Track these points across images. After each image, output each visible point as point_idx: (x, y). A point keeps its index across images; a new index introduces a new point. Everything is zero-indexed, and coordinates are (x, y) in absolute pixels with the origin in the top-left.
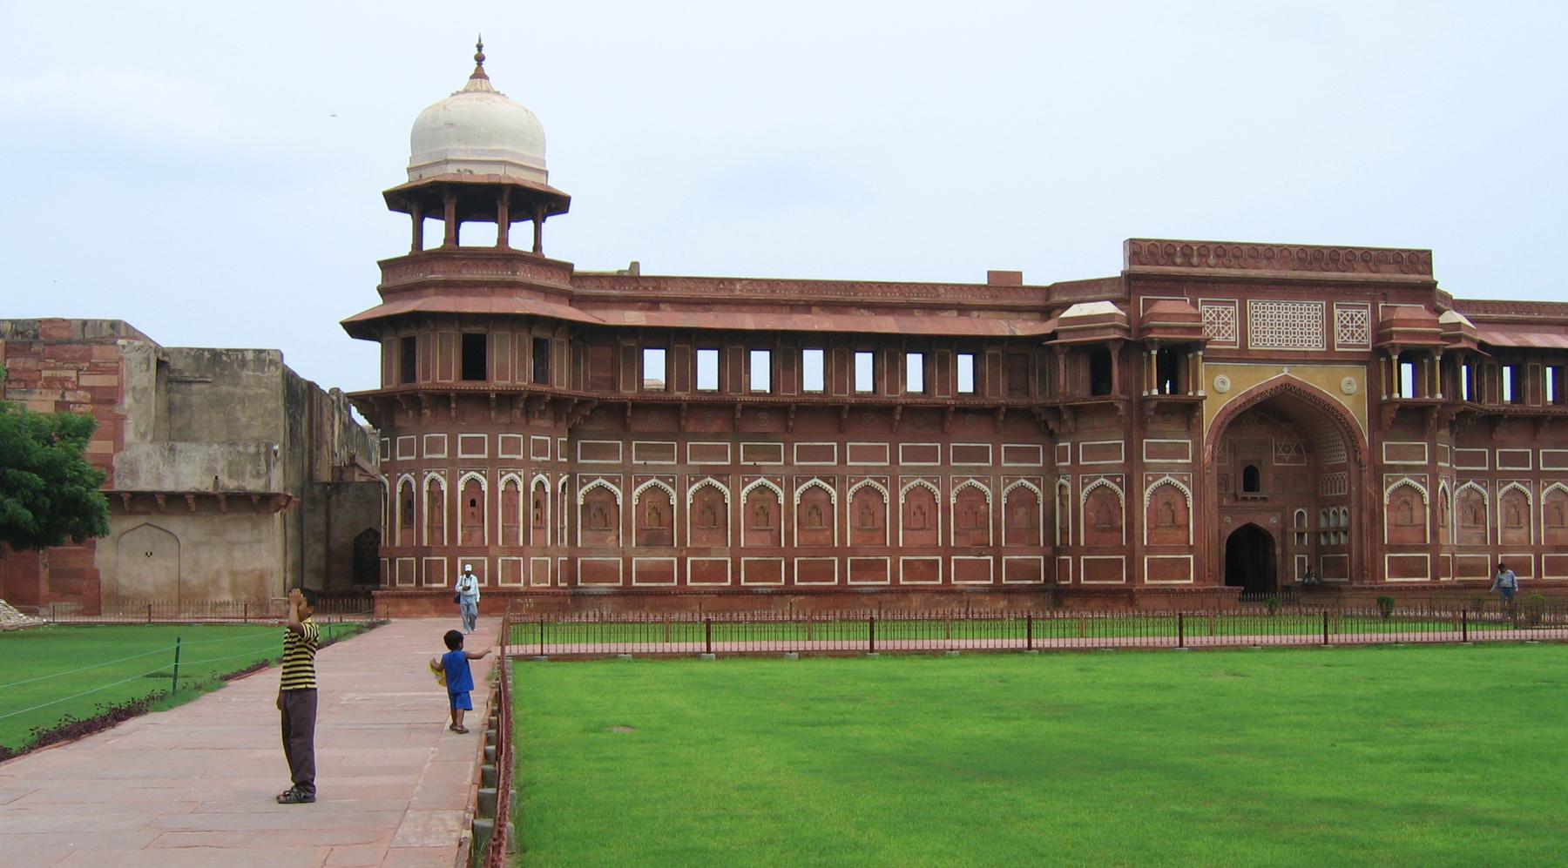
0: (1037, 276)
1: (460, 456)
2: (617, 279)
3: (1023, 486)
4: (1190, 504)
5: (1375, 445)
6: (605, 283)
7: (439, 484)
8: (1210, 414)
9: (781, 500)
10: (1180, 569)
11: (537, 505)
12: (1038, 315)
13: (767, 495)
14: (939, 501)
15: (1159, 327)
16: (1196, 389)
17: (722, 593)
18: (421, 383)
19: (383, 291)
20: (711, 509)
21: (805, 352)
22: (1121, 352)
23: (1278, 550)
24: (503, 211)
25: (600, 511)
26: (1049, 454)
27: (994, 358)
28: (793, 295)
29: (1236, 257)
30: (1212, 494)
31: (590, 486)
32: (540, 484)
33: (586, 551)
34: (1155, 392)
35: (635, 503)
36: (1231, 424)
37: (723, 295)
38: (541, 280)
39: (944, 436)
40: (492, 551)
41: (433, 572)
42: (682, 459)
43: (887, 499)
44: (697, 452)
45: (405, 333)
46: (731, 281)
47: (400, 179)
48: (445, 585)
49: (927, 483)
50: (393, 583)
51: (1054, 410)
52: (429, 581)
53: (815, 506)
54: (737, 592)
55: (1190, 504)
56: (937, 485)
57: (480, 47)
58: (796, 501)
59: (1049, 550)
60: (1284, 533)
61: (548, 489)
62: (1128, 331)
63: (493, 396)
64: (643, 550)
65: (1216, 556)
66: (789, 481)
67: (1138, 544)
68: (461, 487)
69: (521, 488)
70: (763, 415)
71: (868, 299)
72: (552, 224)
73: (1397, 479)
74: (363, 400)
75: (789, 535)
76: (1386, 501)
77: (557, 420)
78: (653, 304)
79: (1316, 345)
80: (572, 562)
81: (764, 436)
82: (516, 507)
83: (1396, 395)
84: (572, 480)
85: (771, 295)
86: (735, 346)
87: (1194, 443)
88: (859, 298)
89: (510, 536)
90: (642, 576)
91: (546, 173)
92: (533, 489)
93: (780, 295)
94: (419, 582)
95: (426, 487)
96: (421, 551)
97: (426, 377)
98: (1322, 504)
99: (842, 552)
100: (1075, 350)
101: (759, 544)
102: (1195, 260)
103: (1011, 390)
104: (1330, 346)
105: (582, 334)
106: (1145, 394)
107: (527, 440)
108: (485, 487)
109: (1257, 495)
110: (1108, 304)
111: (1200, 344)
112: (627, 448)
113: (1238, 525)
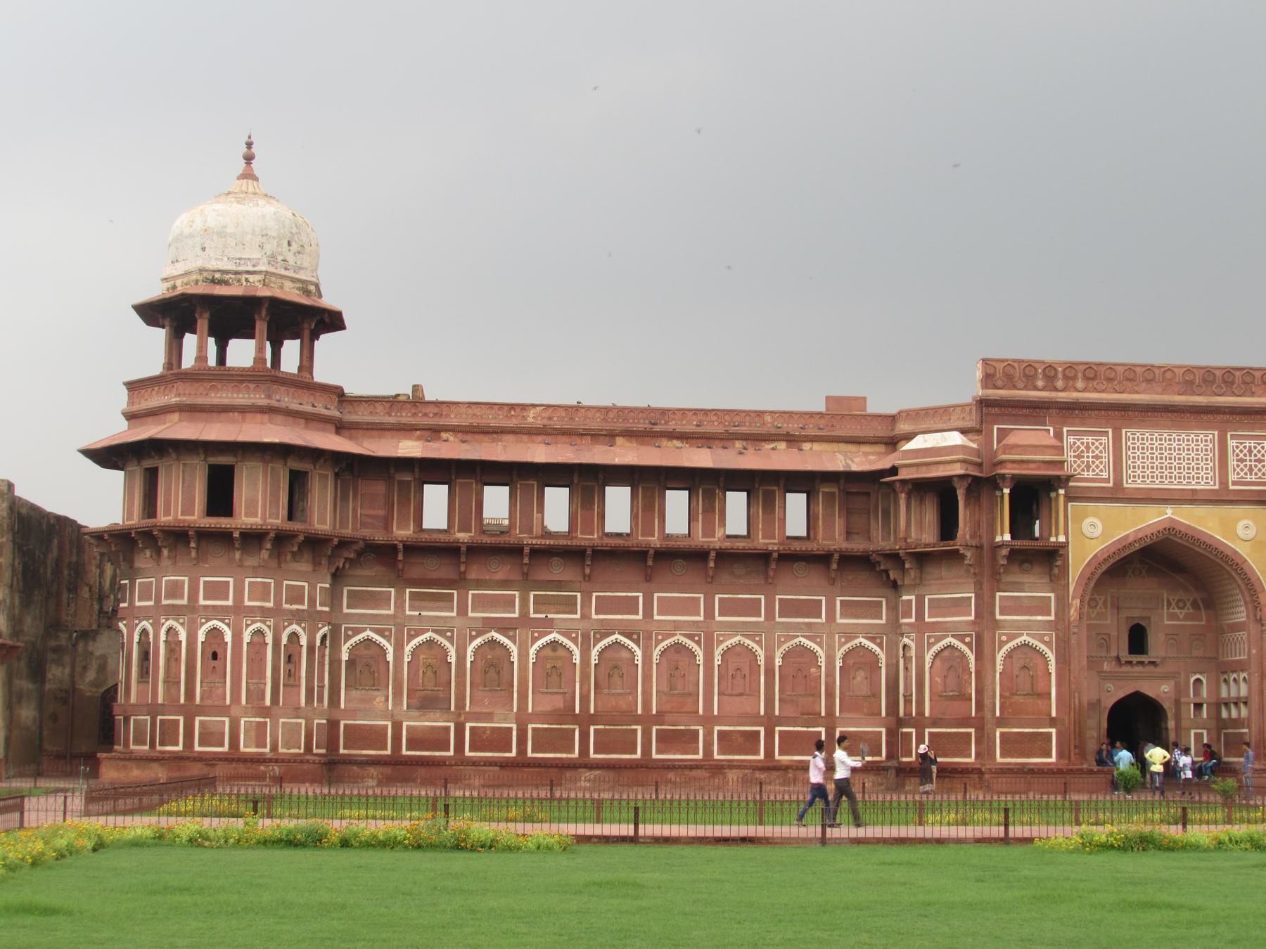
0: (883, 401)
1: (202, 602)
2: (393, 402)
3: (861, 646)
4: (1052, 668)
6: (379, 408)
7: (177, 633)
8: (1079, 562)
9: (577, 658)
10: (1039, 744)
11: (289, 659)
12: (881, 448)
13: (561, 652)
14: (762, 663)
15: (1013, 462)
16: (1057, 536)
17: (505, 764)
18: (163, 518)
19: (131, 416)
20: (493, 667)
21: (610, 491)
22: (969, 491)
23: (1171, 724)
24: (261, 327)
25: (367, 667)
26: (893, 608)
27: (829, 497)
28: (595, 424)
29: (1110, 380)
30: (1079, 660)
31: (356, 639)
32: (294, 637)
33: (351, 713)
34: (1007, 537)
35: (407, 659)
36: (1104, 573)
37: (511, 423)
38: (305, 405)
39: (769, 586)
40: (235, 711)
41: (169, 733)
42: (462, 611)
43: (700, 659)
44: (480, 603)
45: (148, 463)
46: (524, 407)
47: (155, 291)
48: (180, 748)
49: (747, 642)
50: (127, 744)
51: (894, 557)
52: (162, 744)
53: (614, 667)
54: (521, 763)
55: (1052, 668)
56: (759, 643)
57: (249, 145)
58: (594, 659)
59: (892, 719)
60: (1177, 703)
61: (304, 641)
62: (979, 465)
63: (236, 535)
64: (416, 713)
65: (1096, 727)
66: (586, 637)
67: (988, 715)
68: (201, 637)
69: (269, 639)
70: (555, 560)
71: (679, 429)
72: (326, 343)
74: (99, 536)
75: (585, 699)
77: (316, 564)
78: (435, 432)
79: (1206, 482)
80: (333, 725)
81: (559, 585)
82: (263, 660)
84: (335, 631)
85: (649, 424)
86: (527, 478)
87: (1057, 598)
88: (671, 426)
89: (256, 695)
90: (412, 744)
91: (317, 286)
92: (284, 640)
93: (578, 423)
94: (153, 745)
95: (163, 637)
96: (154, 710)
97: (167, 513)
98: (1223, 669)
99: (647, 720)
100: (920, 488)
101: (549, 708)
102: (1060, 384)
103: (849, 534)
105: (352, 468)
106: (998, 539)
107: (278, 586)
108: (228, 638)
110: (956, 434)
111: (1062, 481)
112: (400, 597)
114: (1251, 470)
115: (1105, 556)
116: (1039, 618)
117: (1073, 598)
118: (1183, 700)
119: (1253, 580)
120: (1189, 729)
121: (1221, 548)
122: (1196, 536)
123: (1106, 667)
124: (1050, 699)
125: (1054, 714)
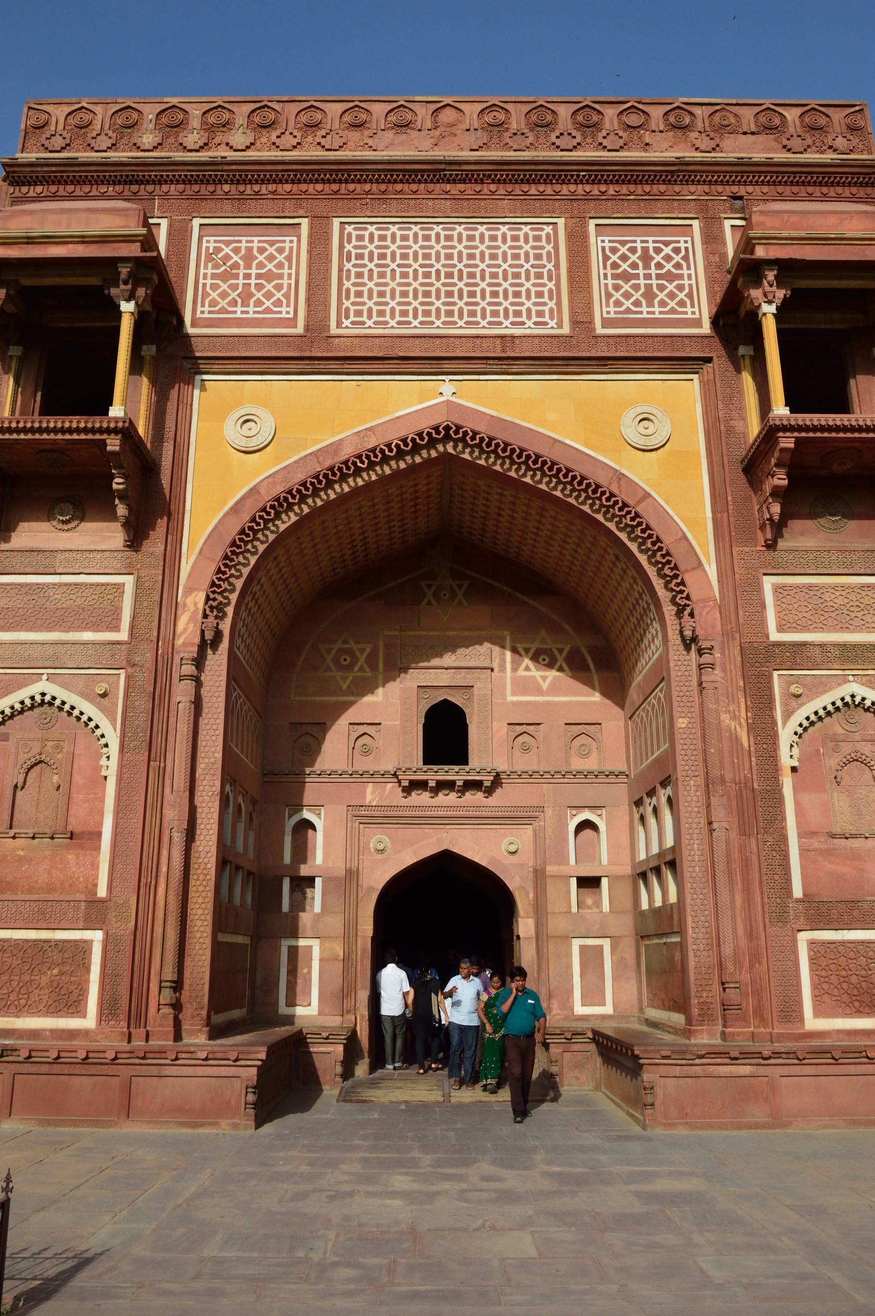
4: (111, 767)
5: (742, 592)
23: (525, 926)
60: (539, 876)
73: (820, 687)
76: (787, 757)
83: (780, 410)
104: (582, 321)
109: (454, 773)
113: (408, 858)
114: (649, 295)
115: (278, 489)
116: (88, 636)
117: (189, 591)
118: (550, 869)
119: (668, 541)
120: (567, 938)
121: (580, 469)
122: (517, 442)
123: (371, 795)
124: (98, 848)
125: (102, 892)
